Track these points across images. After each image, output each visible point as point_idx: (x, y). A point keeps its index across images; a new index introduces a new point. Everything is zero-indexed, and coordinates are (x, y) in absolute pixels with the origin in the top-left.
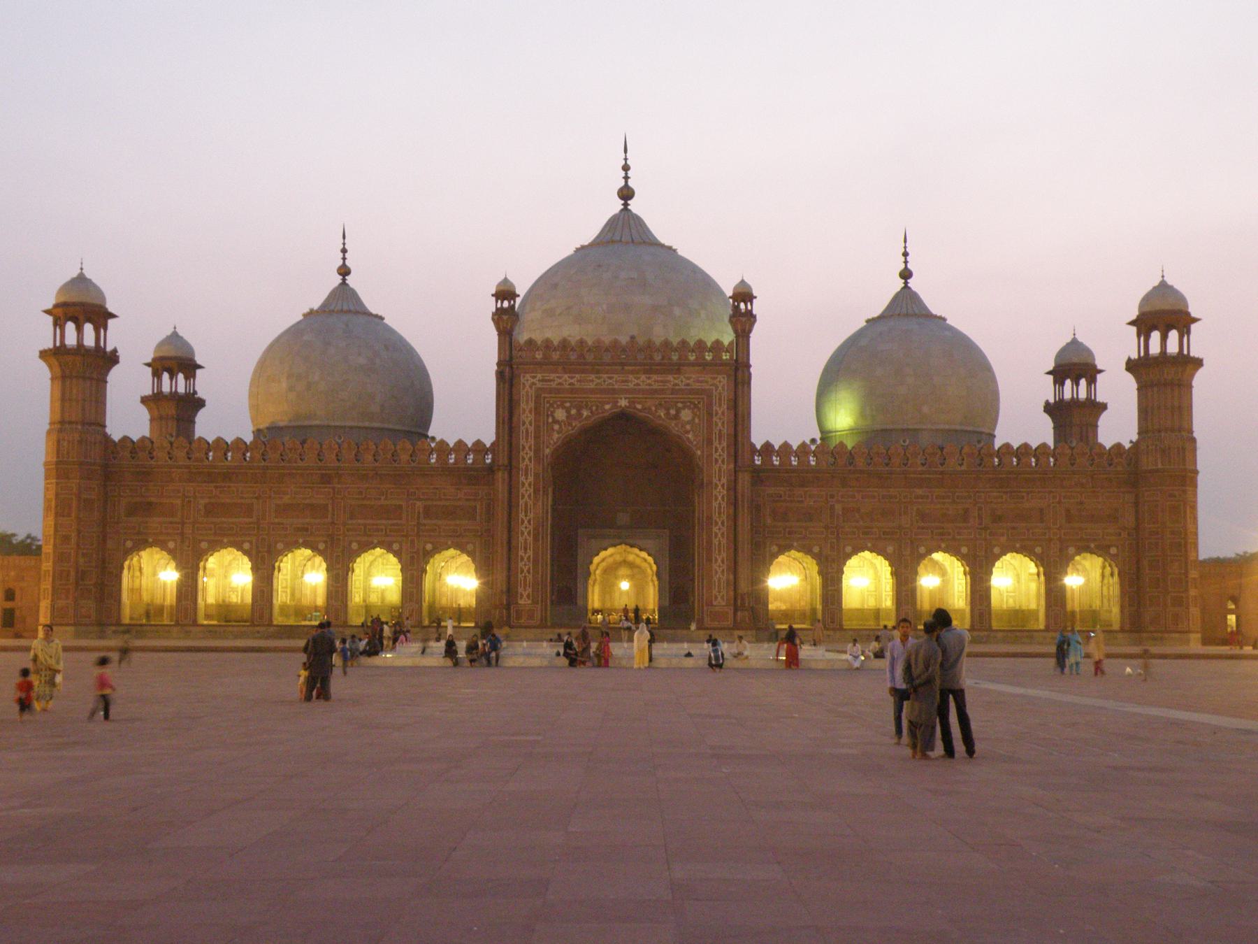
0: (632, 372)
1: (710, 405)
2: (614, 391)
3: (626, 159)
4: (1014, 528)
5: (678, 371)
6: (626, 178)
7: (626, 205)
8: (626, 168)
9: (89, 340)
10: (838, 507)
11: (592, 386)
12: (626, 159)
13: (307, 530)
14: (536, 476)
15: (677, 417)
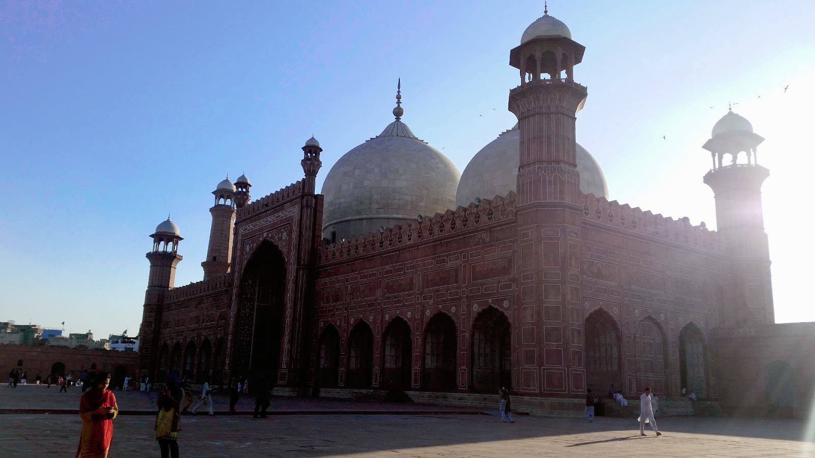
0: (270, 215)
1: (291, 226)
2: (261, 229)
3: (399, 92)
4: (438, 290)
5: (283, 209)
6: (399, 103)
7: (398, 119)
8: (399, 97)
9: (170, 248)
10: (349, 287)
11: (257, 227)
12: (399, 92)
13: (193, 330)
14: (237, 287)
15: (280, 239)
